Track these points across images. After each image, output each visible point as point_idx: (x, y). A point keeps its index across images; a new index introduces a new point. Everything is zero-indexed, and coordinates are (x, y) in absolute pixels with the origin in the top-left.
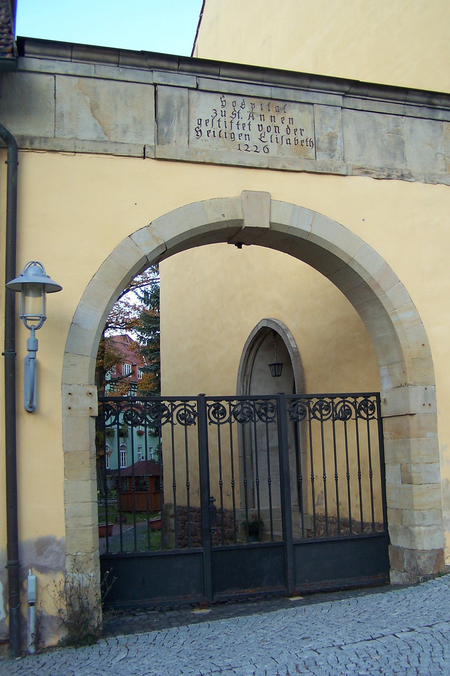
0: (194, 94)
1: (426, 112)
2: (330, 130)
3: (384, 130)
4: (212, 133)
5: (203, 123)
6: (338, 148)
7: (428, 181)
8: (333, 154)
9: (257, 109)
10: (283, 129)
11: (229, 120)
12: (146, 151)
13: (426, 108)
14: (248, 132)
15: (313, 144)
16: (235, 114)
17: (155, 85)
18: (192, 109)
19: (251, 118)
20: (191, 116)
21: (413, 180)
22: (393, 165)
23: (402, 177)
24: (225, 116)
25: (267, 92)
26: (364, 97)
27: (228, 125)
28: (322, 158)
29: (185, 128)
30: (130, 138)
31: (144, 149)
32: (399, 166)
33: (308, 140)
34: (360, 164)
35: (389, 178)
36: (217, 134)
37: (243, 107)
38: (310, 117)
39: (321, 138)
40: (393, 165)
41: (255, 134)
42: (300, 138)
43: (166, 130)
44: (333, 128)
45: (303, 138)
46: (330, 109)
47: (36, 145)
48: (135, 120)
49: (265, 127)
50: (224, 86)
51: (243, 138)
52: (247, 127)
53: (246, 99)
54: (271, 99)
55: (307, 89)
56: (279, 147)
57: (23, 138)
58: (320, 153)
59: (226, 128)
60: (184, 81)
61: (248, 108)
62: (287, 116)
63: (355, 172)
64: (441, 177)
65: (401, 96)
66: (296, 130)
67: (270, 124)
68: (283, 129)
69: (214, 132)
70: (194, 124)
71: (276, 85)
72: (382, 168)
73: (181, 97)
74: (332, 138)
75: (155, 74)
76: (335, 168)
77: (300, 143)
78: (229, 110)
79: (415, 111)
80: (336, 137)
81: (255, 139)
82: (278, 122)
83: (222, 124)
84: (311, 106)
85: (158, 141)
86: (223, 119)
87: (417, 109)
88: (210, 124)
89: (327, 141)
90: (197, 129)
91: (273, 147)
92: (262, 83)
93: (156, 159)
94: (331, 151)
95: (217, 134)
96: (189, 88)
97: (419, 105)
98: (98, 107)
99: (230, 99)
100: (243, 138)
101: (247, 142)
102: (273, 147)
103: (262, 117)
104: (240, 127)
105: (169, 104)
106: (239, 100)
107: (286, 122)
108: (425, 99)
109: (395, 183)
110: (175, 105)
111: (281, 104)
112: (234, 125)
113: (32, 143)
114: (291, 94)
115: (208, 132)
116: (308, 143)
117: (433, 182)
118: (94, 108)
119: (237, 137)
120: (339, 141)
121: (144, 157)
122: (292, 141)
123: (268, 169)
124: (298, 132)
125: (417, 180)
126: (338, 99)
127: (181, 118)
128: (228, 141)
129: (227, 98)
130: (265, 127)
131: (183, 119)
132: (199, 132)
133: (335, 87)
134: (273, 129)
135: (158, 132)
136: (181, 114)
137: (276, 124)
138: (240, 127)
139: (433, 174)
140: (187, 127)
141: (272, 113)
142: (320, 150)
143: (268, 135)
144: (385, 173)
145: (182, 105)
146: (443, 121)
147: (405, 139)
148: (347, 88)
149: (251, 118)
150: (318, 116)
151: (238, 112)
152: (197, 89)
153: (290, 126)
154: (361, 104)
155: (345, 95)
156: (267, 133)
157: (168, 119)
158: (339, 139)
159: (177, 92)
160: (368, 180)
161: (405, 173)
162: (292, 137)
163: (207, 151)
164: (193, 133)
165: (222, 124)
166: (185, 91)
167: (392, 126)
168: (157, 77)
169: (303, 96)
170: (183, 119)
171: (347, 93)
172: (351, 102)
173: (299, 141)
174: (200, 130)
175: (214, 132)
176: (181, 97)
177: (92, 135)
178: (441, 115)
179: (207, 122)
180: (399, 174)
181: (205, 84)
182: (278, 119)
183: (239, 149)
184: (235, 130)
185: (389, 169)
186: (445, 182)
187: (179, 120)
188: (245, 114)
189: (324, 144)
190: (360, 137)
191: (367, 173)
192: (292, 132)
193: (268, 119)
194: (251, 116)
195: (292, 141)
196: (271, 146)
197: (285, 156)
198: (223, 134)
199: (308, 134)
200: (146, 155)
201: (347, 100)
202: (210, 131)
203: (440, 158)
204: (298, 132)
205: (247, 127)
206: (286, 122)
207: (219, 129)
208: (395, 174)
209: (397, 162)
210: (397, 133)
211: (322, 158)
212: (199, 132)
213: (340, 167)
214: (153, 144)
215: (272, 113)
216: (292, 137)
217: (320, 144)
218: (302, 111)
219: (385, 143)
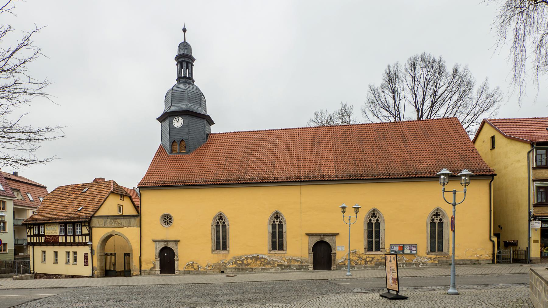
15: (120, 224)
23: (130, 227)
25: (115, 218)
30: (102, 225)
57: (93, 227)
74: (122, 223)
79: (132, 217)
81: (114, 224)
85: (104, 226)
91: (116, 225)
114: (117, 218)
118: (98, 222)
169: (118, 218)
177: (98, 226)
178: (135, 217)
188: (113, 221)
190: (125, 222)
191: (126, 227)
199: (119, 223)
210: (130, 221)
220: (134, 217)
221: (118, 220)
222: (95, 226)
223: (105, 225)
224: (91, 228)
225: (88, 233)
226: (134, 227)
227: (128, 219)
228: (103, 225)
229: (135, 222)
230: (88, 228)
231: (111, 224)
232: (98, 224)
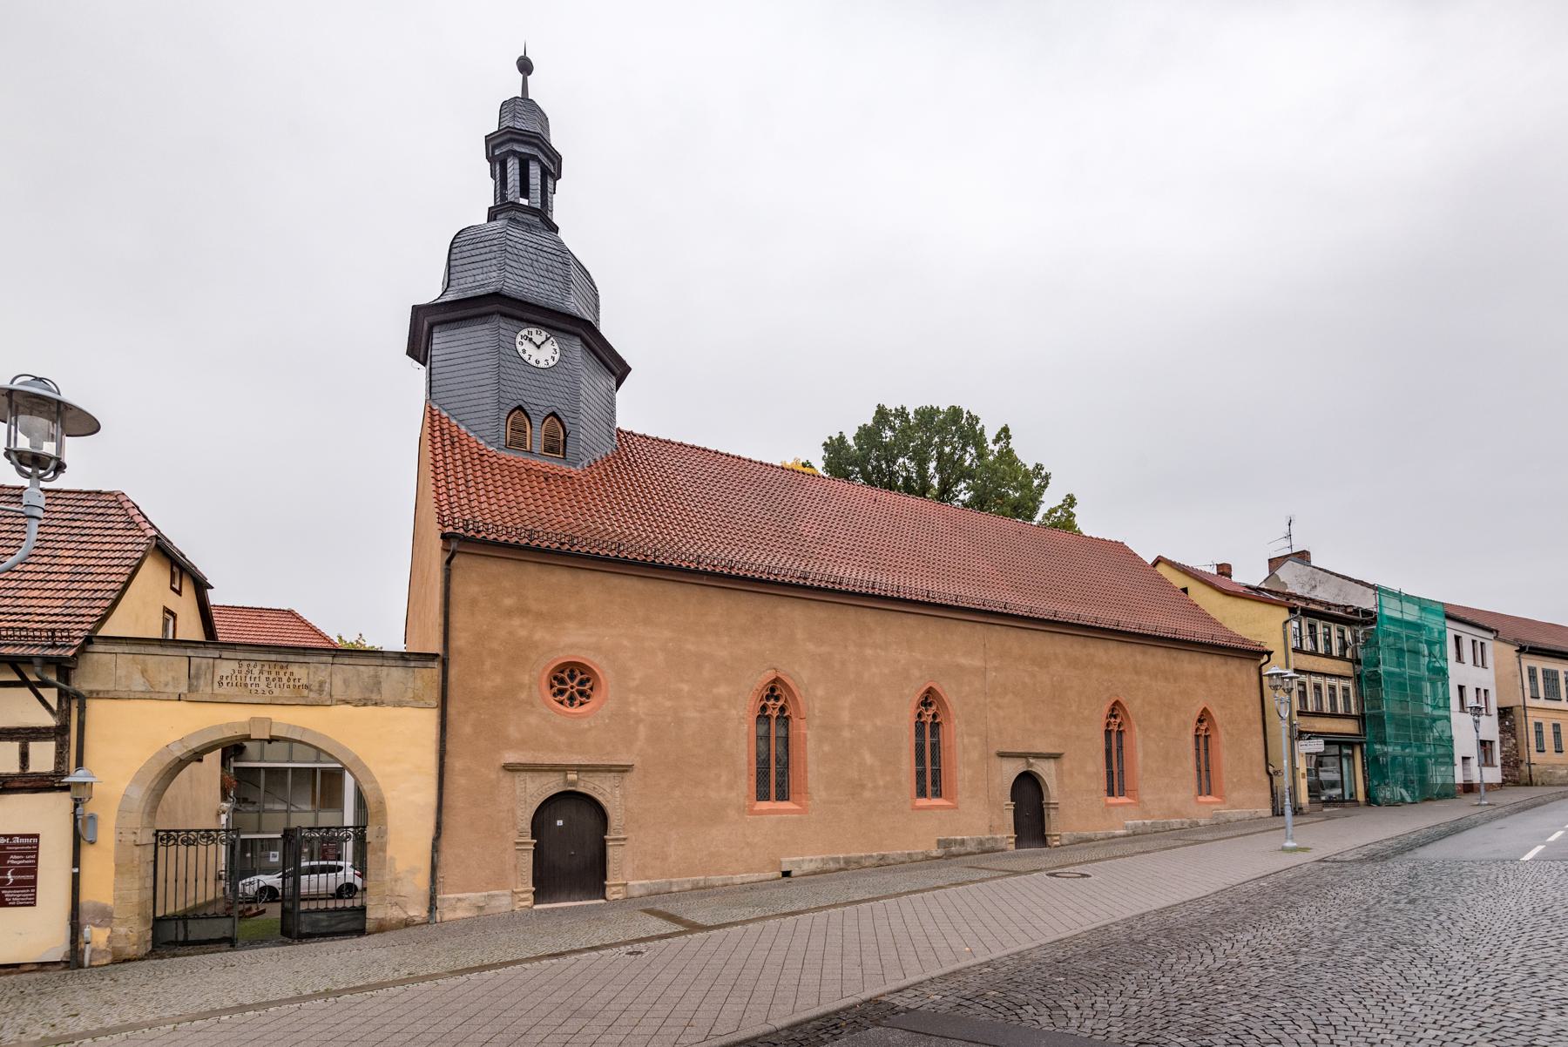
0: (218, 661)
1: (400, 663)
5: (224, 678)
9: (266, 668)
10: (285, 679)
11: (243, 675)
17: (189, 657)
23: (376, 704)
25: (273, 657)
26: (351, 657)
29: (210, 682)
30: (170, 689)
32: (375, 697)
34: (343, 698)
35: (365, 705)
36: (234, 684)
41: (263, 685)
42: (297, 684)
46: (323, 666)
47: (101, 695)
48: (173, 678)
49: (271, 679)
50: (240, 656)
52: (257, 679)
55: (304, 655)
61: (259, 668)
62: (289, 671)
68: (285, 679)
70: (217, 679)
71: (280, 653)
73: (208, 664)
74: (321, 684)
75: (188, 650)
76: (322, 702)
78: (244, 669)
83: (239, 678)
86: (239, 675)
88: (229, 679)
89: (317, 685)
91: (277, 692)
94: (321, 690)
95: (234, 684)
98: (146, 671)
99: (245, 663)
102: (277, 692)
103: (269, 673)
104: (253, 679)
105: (199, 667)
106: (253, 663)
107: (288, 675)
111: (285, 665)
112: (248, 679)
113: (98, 694)
114: (291, 658)
115: (228, 684)
117: (400, 706)
118: (144, 672)
121: (179, 700)
122: (291, 687)
123: (270, 704)
126: (330, 659)
127: (207, 676)
128: (243, 689)
129: (242, 662)
130: (271, 679)
131: (209, 676)
132: (220, 684)
134: (277, 679)
138: (253, 679)
145: (209, 668)
147: (382, 680)
152: (220, 658)
153: (291, 677)
154: (347, 661)
157: (198, 677)
159: (205, 661)
160: (349, 707)
161: (379, 701)
162: (292, 683)
164: (216, 685)
165: (239, 678)
166: (211, 660)
168: (189, 652)
169: (301, 659)
176: (208, 664)
177: (143, 689)
178: (412, 664)
181: (225, 654)
184: (248, 681)
188: (256, 671)
190: (346, 682)
191: (348, 703)
192: (292, 680)
194: (261, 672)
195: (291, 687)
198: (239, 684)
199: (304, 681)
205: (257, 679)
206: (288, 675)
212: (220, 684)
214: (186, 692)
216: (292, 683)
218: (301, 668)
220: (407, 660)
221: (295, 669)
222: (110, 687)
223: (191, 688)
224: (82, 699)
225: (50, 721)
226: (399, 704)
227: (362, 668)
228: (184, 689)
230: (51, 695)
231: (246, 685)
232: (138, 677)
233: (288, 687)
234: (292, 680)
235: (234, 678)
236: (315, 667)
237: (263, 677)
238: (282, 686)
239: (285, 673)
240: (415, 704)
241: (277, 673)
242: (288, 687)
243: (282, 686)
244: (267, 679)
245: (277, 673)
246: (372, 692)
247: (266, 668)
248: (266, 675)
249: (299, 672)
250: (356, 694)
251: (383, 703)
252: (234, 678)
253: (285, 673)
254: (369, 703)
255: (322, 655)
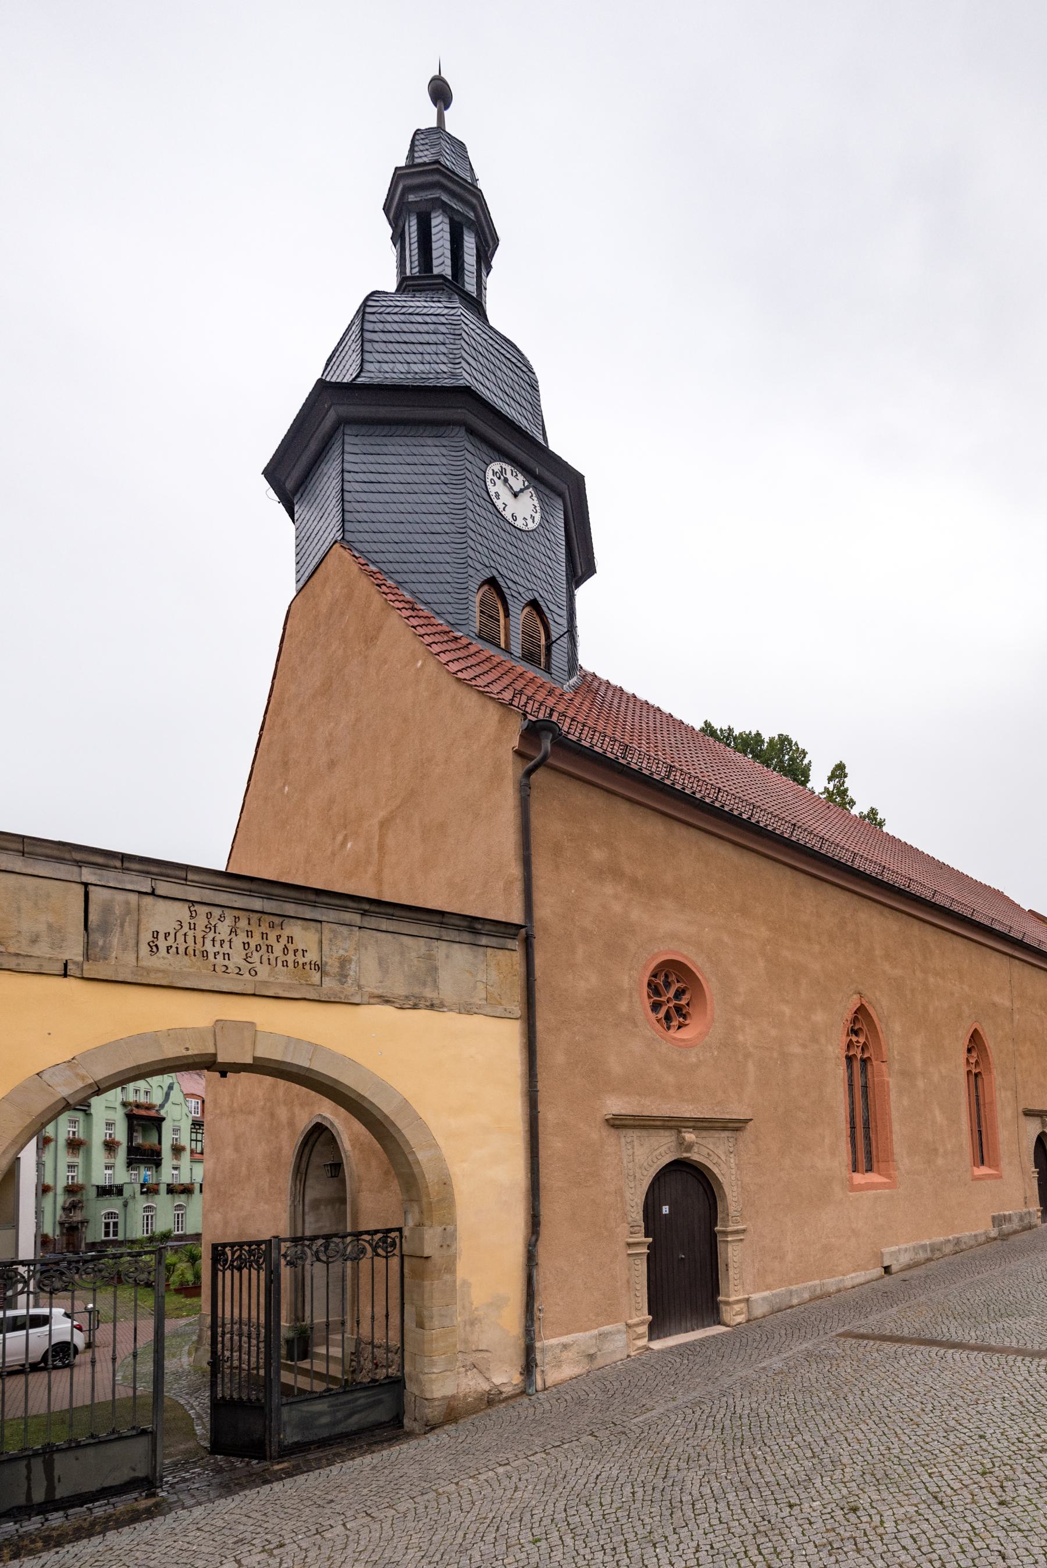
0: (148, 900)
1: (466, 937)
2: (341, 952)
3: (414, 954)
4: (174, 950)
5: (161, 936)
6: (352, 973)
7: (463, 1011)
8: (344, 980)
9: (243, 924)
10: (278, 949)
11: (199, 934)
12: (69, 967)
13: (467, 933)
14: (228, 951)
16: (211, 928)
17: (86, 885)
18: (144, 919)
19: (233, 934)
20: (142, 927)
21: (445, 1010)
22: (421, 993)
23: (432, 1007)
24: (195, 929)
26: (390, 917)
27: (199, 940)
28: (329, 983)
29: (132, 942)
30: (42, 949)
31: (66, 965)
32: (429, 993)
33: (313, 963)
35: (415, 1007)
36: (181, 950)
37: (222, 919)
38: (316, 937)
39: (330, 962)
40: (421, 993)
42: (301, 960)
43: (101, 943)
44: (346, 951)
45: (305, 960)
46: (344, 930)
51: (220, 957)
52: (226, 945)
53: (227, 912)
54: (263, 912)
55: (314, 905)
56: (272, 970)
58: (327, 979)
59: (195, 943)
60: (131, 882)
61: (228, 922)
62: (286, 932)
63: (372, 1001)
64: (479, 1007)
65: (437, 918)
66: (296, 951)
67: (261, 942)
68: (278, 949)
69: (177, 948)
70: (146, 937)
71: (270, 897)
72: (407, 997)
74: (344, 962)
77: (301, 966)
79: (453, 935)
80: (350, 961)
82: (272, 939)
83: (190, 939)
84: (319, 925)
85: (87, 956)
86: (191, 933)
87: (456, 932)
88: (171, 938)
89: (337, 964)
90: (151, 944)
92: (251, 893)
93: (83, 978)
95: (181, 950)
96: (140, 893)
97: (458, 928)
100: (220, 957)
101: (226, 962)
103: (249, 933)
104: (217, 944)
107: (283, 941)
108: (465, 924)
109: (423, 1014)
110: (117, 912)
111: (277, 920)
115: (169, 948)
116: (313, 966)
117: (469, 1012)
119: (211, 956)
120: (353, 966)
123: (254, 995)
124: (300, 953)
125: (451, 1010)
126: (356, 918)
127: (127, 929)
128: (198, 961)
129: (197, 907)
131: (130, 930)
132: (154, 948)
133: (350, 904)
134: (264, 948)
135: (87, 945)
136: (126, 924)
137: (268, 942)
138: (217, 944)
139: (470, 1004)
140: (134, 941)
141: (264, 928)
142: (328, 974)
143: (256, 957)
144: (411, 1003)
146: (487, 947)
147: (439, 964)
148: (367, 907)
149: (233, 934)
150: (327, 935)
151: (215, 926)
153: (289, 946)
154: (385, 924)
155: (364, 913)
156: (255, 953)
157: (105, 928)
158: (353, 963)
159: (120, 897)
163: (163, 971)
164: (144, 949)
165: (190, 939)
167: (423, 950)
169: (308, 913)
170: (130, 930)
171: (366, 911)
172: (371, 922)
173: (301, 963)
174: (156, 946)
175: (177, 948)
176: (127, 903)
178: (484, 941)
179: (167, 935)
180: (428, 1004)
181: (163, 888)
182: (272, 936)
183: (214, 970)
185: (416, 998)
186: (485, 1012)
187: (122, 931)
188: (224, 928)
189: (333, 967)
190: (381, 961)
191: (387, 1002)
192: (291, 953)
193: (257, 936)
194: (234, 931)
196: (259, 967)
197: (279, 981)
198: (190, 951)
199: (313, 956)
200: (68, 973)
201: (367, 918)
202: (171, 947)
203: (481, 986)
204: (300, 953)
205: (226, 945)
207: (185, 946)
208: (422, 1003)
209: (427, 990)
210: (429, 957)
211: (329, 983)
212: (154, 948)
213: (352, 995)
214: (80, 959)
215: (264, 928)
216: (290, 958)
217: (328, 968)
218: (305, 929)
219: (414, 969)
220: (476, 932)
221: (295, 929)
226: (467, 1009)
228: (74, 952)
229: (481, 976)
231: (205, 954)
233: (285, 964)
234: (291, 953)
235: (180, 936)
236: (333, 931)
237: (238, 941)
238: (273, 962)
239: (278, 937)
240: (488, 1010)
241: (264, 936)
242: (285, 964)
243: (273, 962)
244: (246, 945)
245: (264, 936)
246: (424, 984)
247: (243, 924)
248: (242, 937)
249: (304, 937)
250: (400, 989)
251: (442, 1005)
252: (180, 936)
253: (278, 937)
254: (422, 1003)
255: (345, 909)
